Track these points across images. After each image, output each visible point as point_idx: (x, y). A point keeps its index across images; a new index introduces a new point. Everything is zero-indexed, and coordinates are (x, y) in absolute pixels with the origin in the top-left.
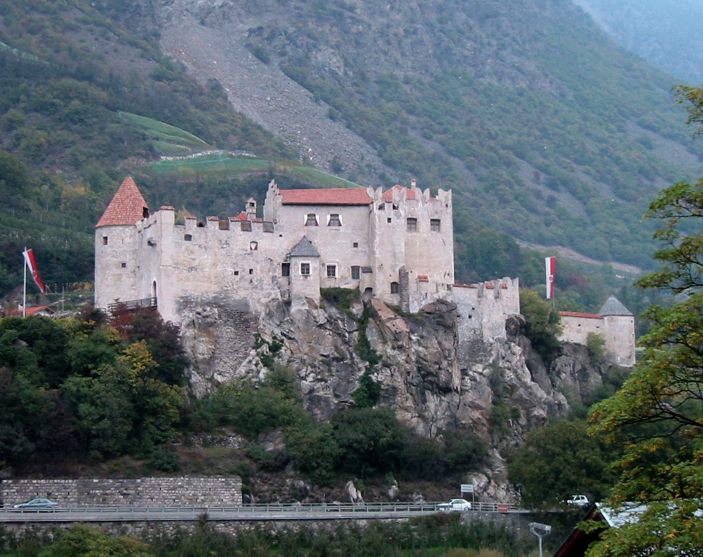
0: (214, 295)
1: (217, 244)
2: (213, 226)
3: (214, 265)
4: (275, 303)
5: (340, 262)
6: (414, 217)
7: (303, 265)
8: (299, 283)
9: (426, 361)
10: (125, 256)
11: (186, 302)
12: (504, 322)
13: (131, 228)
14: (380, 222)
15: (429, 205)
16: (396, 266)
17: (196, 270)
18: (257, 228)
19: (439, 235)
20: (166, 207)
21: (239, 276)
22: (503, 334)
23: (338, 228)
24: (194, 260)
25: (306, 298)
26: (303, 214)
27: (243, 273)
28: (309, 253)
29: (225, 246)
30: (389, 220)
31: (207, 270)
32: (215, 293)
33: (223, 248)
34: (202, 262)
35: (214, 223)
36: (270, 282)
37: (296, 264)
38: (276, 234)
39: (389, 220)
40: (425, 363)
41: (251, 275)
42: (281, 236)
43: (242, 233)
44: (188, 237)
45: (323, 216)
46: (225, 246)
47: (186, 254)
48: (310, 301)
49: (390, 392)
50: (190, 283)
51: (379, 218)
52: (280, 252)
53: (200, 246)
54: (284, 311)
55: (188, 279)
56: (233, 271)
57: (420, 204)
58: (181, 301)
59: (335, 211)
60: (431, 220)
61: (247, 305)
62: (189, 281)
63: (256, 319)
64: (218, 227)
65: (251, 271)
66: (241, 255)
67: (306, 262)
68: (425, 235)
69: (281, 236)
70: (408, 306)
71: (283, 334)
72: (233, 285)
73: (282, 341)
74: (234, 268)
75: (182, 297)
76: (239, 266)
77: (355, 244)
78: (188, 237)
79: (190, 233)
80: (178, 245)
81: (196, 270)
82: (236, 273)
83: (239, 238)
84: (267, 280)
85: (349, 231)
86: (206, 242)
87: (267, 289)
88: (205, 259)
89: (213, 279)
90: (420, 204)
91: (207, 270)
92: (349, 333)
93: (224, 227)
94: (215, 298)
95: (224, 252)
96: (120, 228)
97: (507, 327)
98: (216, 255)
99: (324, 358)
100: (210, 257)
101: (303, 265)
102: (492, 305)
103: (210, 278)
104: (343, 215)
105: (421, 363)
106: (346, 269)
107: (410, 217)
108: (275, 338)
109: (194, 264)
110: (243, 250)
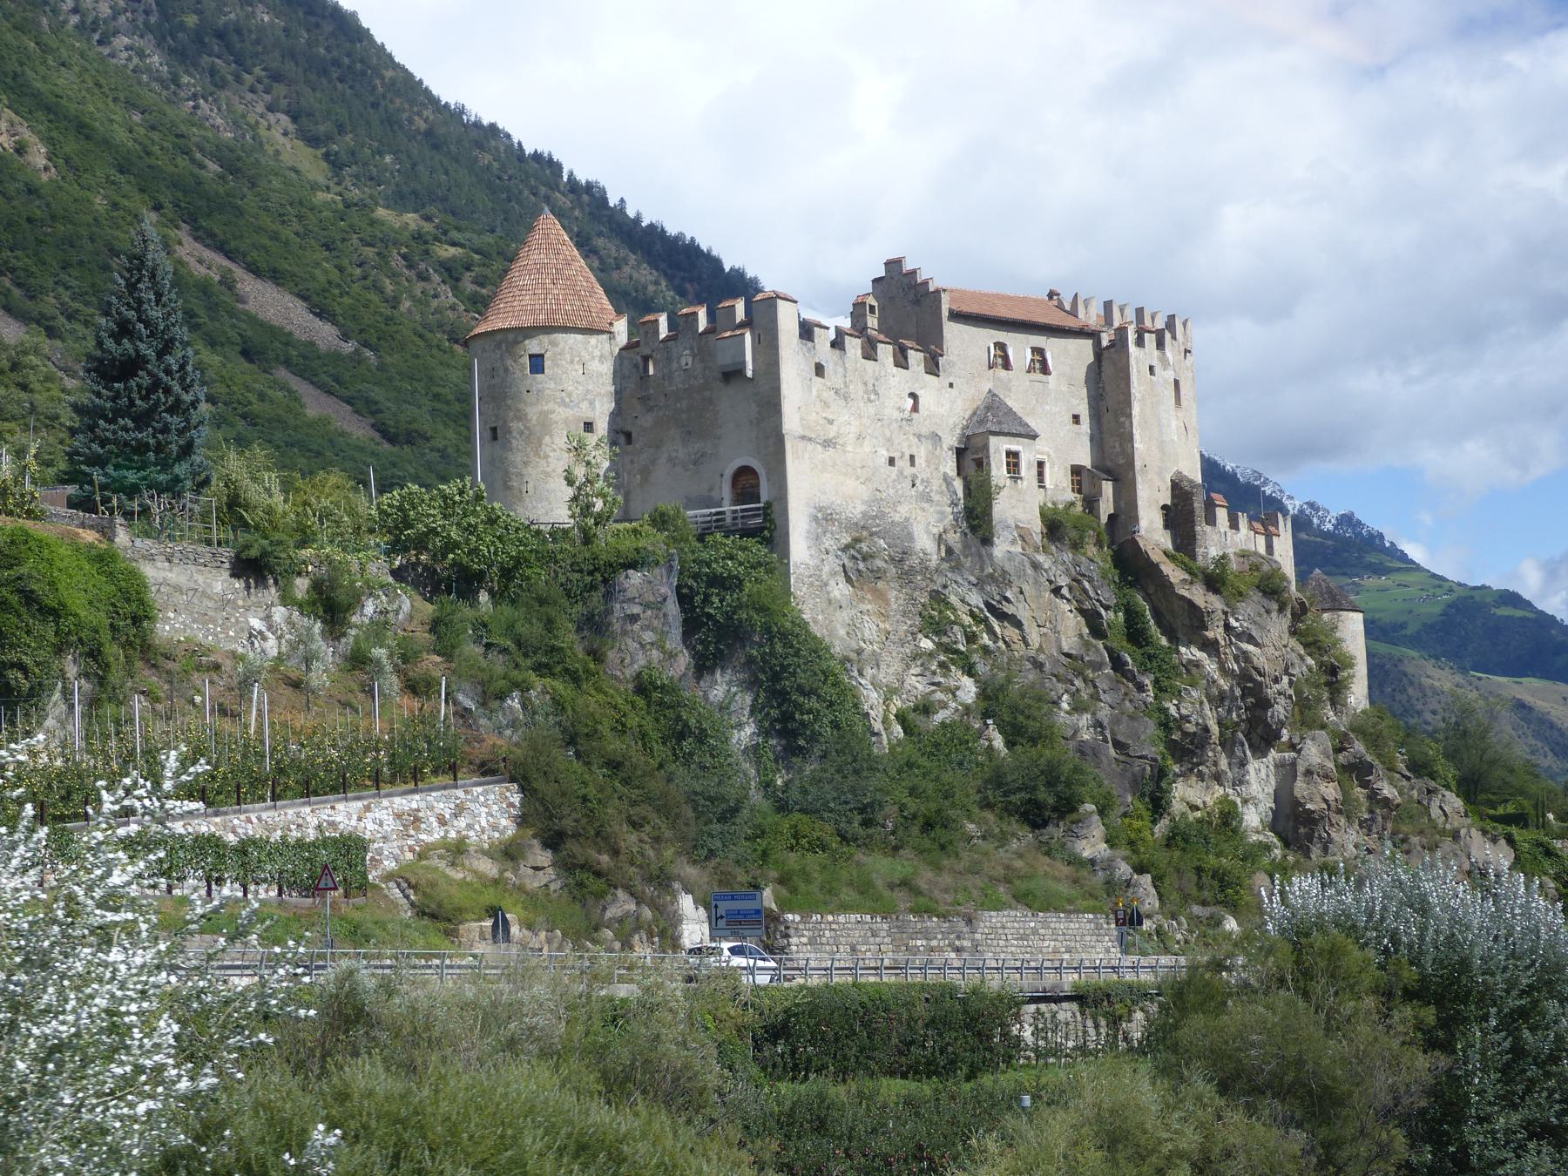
7: (1009, 454)
10: (591, 403)
13: (605, 337)
24: (831, 422)
25: (1017, 527)
26: (989, 337)
28: (1021, 430)
37: (997, 450)
39: (1151, 368)
45: (1020, 347)
52: (951, 422)
59: (1039, 340)
67: (1014, 448)
84: (937, 483)
85: (1064, 388)
94: (864, 514)
95: (871, 410)
96: (579, 337)
101: (1009, 454)
104: (1054, 347)
109: (832, 432)
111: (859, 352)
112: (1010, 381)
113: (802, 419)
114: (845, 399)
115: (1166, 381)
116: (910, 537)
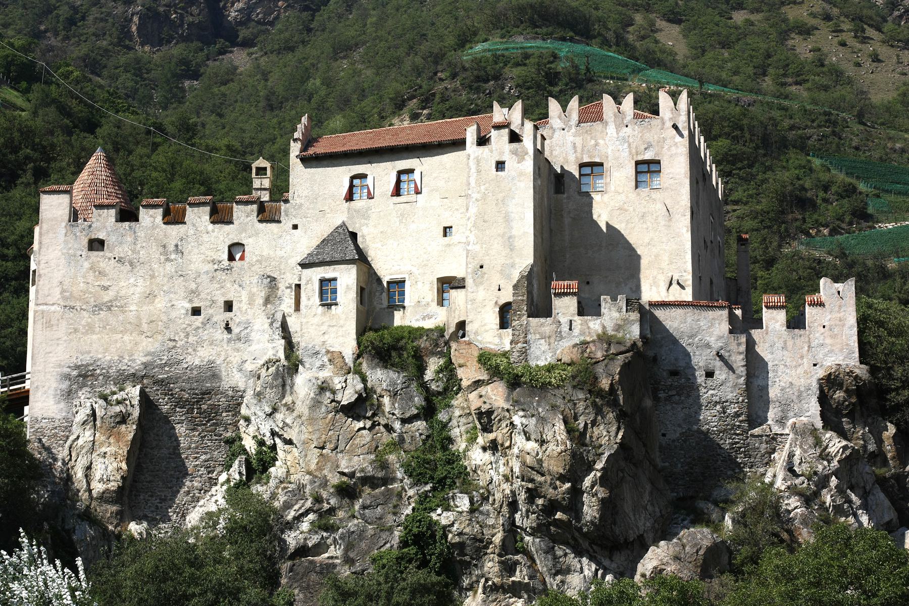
0: (144, 360)
1: (155, 253)
2: (150, 218)
3: (150, 296)
4: (272, 370)
5: (414, 270)
6: (597, 160)
7: (323, 281)
8: (316, 320)
9: (543, 475)
11: (85, 376)
12: (815, 386)
14: (479, 171)
15: (633, 132)
16: (513, 266)
17: (109, 308)
18: (244, 215)
19: (655, 195)
20: (55, 187)
21: (200, 319)
22: (812, 411)
23: (413, 197)
24: (106, 288)
25: (328, 352)
26: (341, 175)
27: (211, 311)
29: (173, 256)
30: (500, 166)
31: (133, 308)
32: (148, 354)
33: (168, 260)
34: (122, 293)
35: (152, 212)
36: (267, 326)
38: (287, 223)
39: (500, 166)
40: (539, 478)
41: (229, 314)
42: (295, 227)
43: (211, 227)
44: (96, 245)
45: (382, 175)
46: (173, 256)
47: (91, 277)
48: (335, 358)
49: (468, 550)
50: (95, 337)
51: (478, 161)
53: (120, 260)
54: (284, 386)
55: (90, 329)
56: (189, 306)
57: (611, 129)
58: (75, 373)
60: (638, 163)
61: (215, 376)
62: (93, 332)
63: (235, 406)
64: (159, 219)
65: (229, 306)
66: (207, 273)
68: (622, 197)
69: (295, 227)
70: (524, 352)
71: (273, 434)
72: (187, 336)
73: (274, 447)
74: (191, 301)
75: (77, 367)
76: (203, 296)
77: (445, 228)
78: (96, 245)
79: (101, 236)
80: (72, 258)
81: (109, 308)
82: (196, 311)
83: (205, 237)
86: (134, 251)
87: (259, 342)
88: (130, 286)
89: (145, 327)
90: (611, 129)
91: (133, 308)
92: (404, 421)
93: (173, 217)
94: (146, 365)
97: (823, 399)
98: (153, 277)
99: (345, 479)
100: (141, 281)
101: (323, 281)
102: (779, 345)
103: (138, 325)
104: (423, 166)
105: (531, 481)
106: (427, 287)
107: (586, 160)
108: (261, 443)
109: (107, 297)
110: (213, 262)
111: (208, 218)
112: (369, 208)
113: (63, 291)
114: (131, 264)
115: (521, 174)
116: (215, 376)
